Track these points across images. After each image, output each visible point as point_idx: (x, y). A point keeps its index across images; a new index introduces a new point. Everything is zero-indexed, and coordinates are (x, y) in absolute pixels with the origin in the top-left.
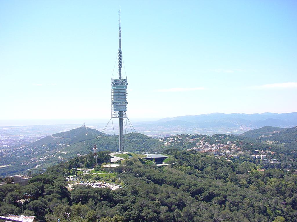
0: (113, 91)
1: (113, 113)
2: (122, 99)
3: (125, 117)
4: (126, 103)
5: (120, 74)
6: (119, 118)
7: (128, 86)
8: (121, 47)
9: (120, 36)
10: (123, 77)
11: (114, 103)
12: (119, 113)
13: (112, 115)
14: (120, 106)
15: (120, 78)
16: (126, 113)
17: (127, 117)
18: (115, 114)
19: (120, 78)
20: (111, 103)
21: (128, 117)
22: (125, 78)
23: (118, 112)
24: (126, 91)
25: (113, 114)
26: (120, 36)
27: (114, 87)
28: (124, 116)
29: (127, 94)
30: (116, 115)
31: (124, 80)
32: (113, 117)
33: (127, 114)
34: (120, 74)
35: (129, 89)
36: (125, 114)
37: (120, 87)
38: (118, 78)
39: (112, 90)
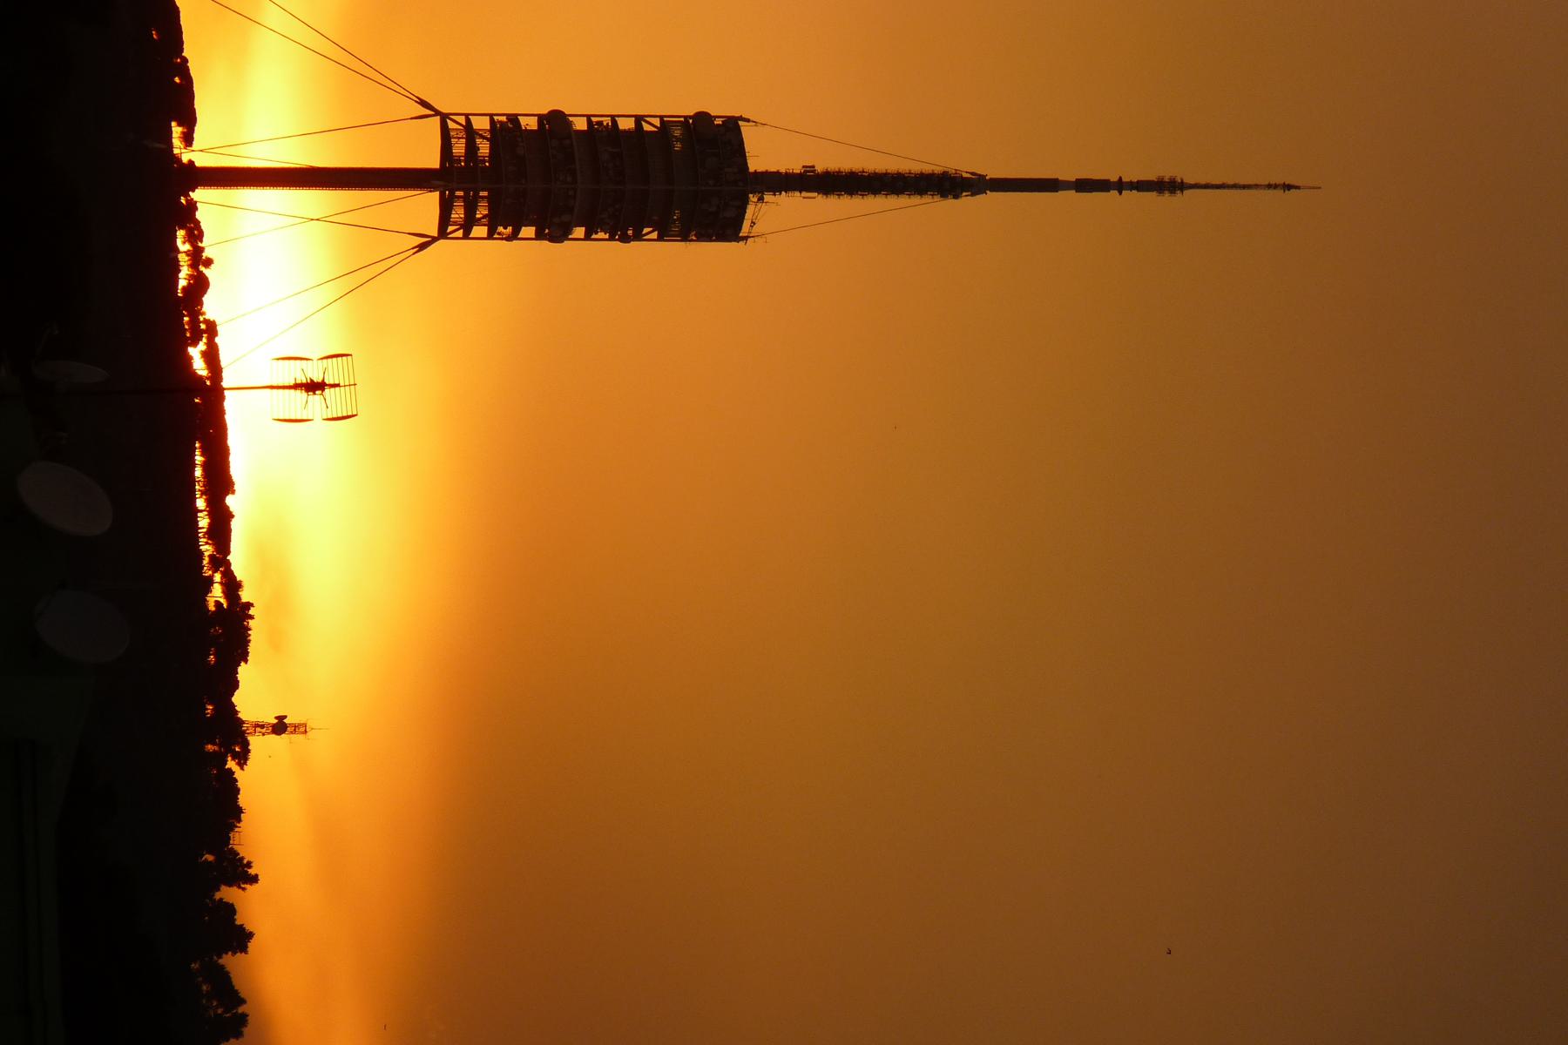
1: (481, 124)
3: (444, 220)
9: (1083, 185)
13: (462, 120)
17: (443, 234)
21: (441, 241)
26: (1083, 185)
32: (451, 125)
33: (466, 236)
36: (467, 226)
38: (755, 164)
39: (657, 122)
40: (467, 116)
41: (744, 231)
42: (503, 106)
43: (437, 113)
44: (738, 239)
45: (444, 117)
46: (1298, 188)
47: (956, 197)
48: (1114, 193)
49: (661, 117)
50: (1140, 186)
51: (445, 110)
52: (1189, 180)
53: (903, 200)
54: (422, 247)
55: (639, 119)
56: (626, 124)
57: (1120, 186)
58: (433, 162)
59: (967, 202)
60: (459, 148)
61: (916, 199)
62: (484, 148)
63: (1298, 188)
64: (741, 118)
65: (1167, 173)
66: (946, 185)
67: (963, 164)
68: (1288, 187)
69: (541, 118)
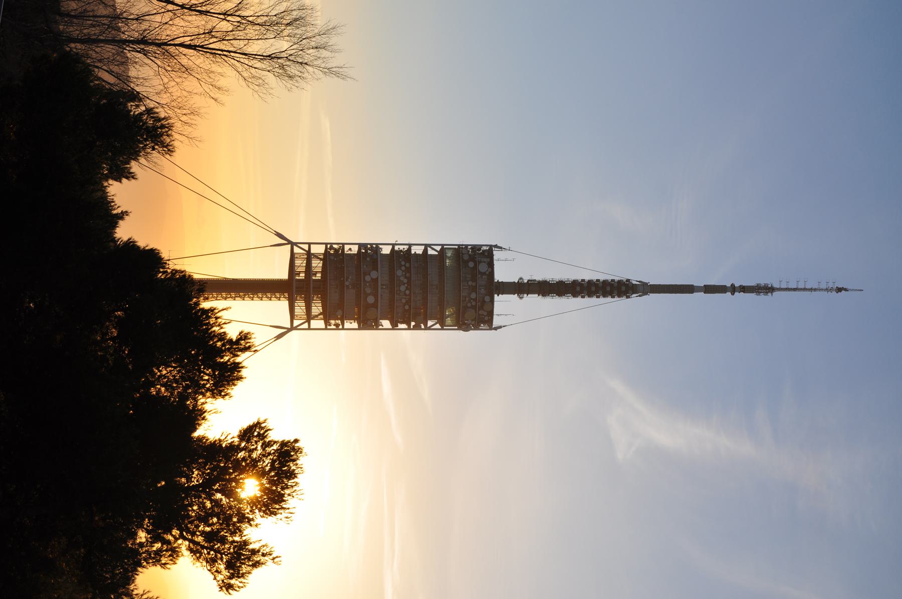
1: (319, 250)
5: (521, 288)
6: (284, 275)
8: (653, 296)
9: (709, 289)
11: (369, 252)
13: (306, 247)
25: (312, 252)
26: (709, 289)
32: (296, 250)
33: (309, 329)
34: (521, 288)
36: (309, 317)
40: (309, 244)
41: (496, 321)
42: (334, 238)
44: (491, 328)
46: (846, 290)
47: (628, 297)
48: (729, 294)
49: (443, 245)
50: (744, 289)
51: (294, 241)
52: (776, 286)
53: (594, 300)
54: (279, 337)
56: (418, 250)
57: (733, 289)
59: (635, 299)
60: (300, 264)
61: (602, 300)
62: (317, 264)
63: (846, 290)
64: (496, 246)
65: (763, 282)
66: (620, 289)
67: (635, 277)
68: (839, 290)
69: (361, 246)
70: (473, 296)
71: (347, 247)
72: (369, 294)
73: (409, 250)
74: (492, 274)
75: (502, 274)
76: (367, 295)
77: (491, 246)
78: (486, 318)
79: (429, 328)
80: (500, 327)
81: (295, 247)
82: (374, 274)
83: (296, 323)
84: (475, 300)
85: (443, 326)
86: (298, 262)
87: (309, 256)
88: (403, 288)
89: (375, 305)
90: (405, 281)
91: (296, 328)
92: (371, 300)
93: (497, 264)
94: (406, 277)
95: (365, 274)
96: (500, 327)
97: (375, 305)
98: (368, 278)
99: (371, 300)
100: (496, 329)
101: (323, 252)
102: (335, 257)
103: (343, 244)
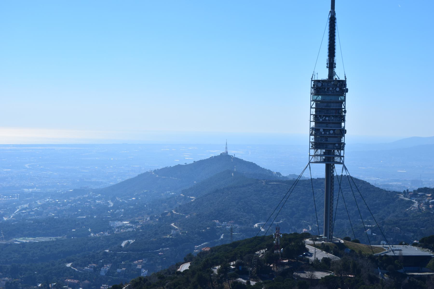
0: (314, 106)
1: (312, 152)
2: (333, 123)
3: (339, 163)
4: (343, 132)
5: (331, 65)
7: (347, 95)
10: (339, 75)
11: (315, 131)
12: (325, 154)
13: (311, 157)
14: (329, 139)
15: (331, 73)
16: (342, 155)
17: (343, 163)
18: (318, 155)
19: (331, 73)
20: (308, 132)
21: (345, 163)
22: (342, 78)
23: (324, 151)
24: (343, 107)
27: (315, 97)
28: (337, 159)
29: (345, 112)
30: (319, 157)
31: (339, 81)
32: (312, 161)
33: (343, 156)
34: (331, 65)
35: (352, 104)
36: (340, 156)
37: (329, 97)
40: (310, 156)
41: (344, 79)
43: (309, 164)
45: (310, 162)
49: (311, 101)
53: (336, 34)
54: (346, 169)
55: (311, 108)
56: (313, 111)
58: (324, 166)
59: (337, 16)
61: (336, 31)
64: (312, 79)
69: (311, 135)
70: (331, 89)
71: (312, 141)
72: (329, 132)
73: (314, 115)
74: (323, 81)
75: (324, 75)
76: (330, 134)
77: (312, 80)
78: (341, 83)
79: (345, 107)
80: (345, 77)
81: (311, 161)
82: (321, 130)
83: (341, 162)
84: (333, 88)
85: (345, 100)
86: (319, 160)
87: (315, 155)
88: (327, 118)
89: (334, 130)
90: (324, 117)
91: (343, 162)
92: (332, 132)
93: (320, 79)
94: (323, 117)
95: (321, 134)
96: (345, 77)
97: (334, 130)
98: (323, 133)
99: (332, 132)
100: (346, 79)
101: (313, 150)
102: (316, 145)
103: (310, 142)
